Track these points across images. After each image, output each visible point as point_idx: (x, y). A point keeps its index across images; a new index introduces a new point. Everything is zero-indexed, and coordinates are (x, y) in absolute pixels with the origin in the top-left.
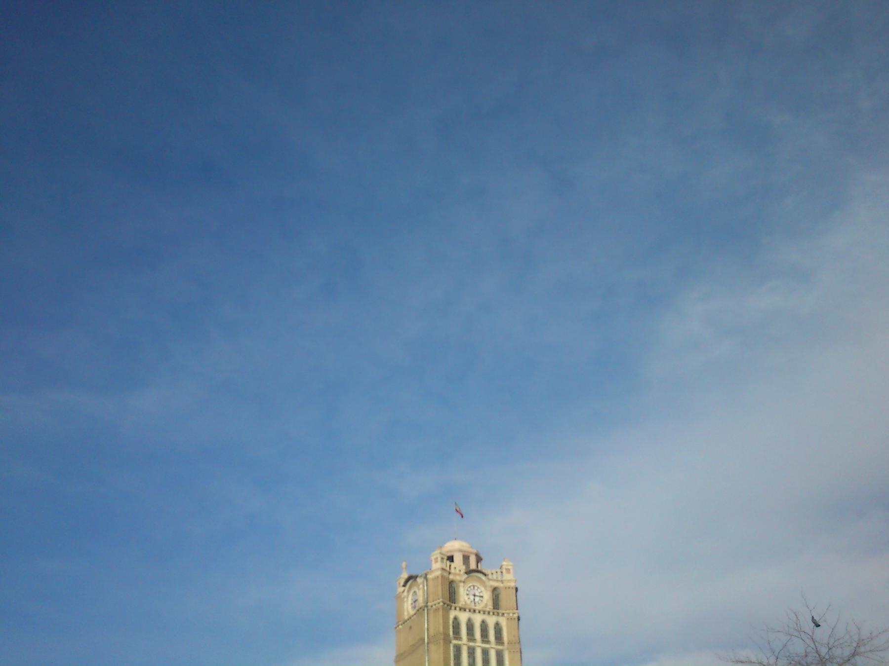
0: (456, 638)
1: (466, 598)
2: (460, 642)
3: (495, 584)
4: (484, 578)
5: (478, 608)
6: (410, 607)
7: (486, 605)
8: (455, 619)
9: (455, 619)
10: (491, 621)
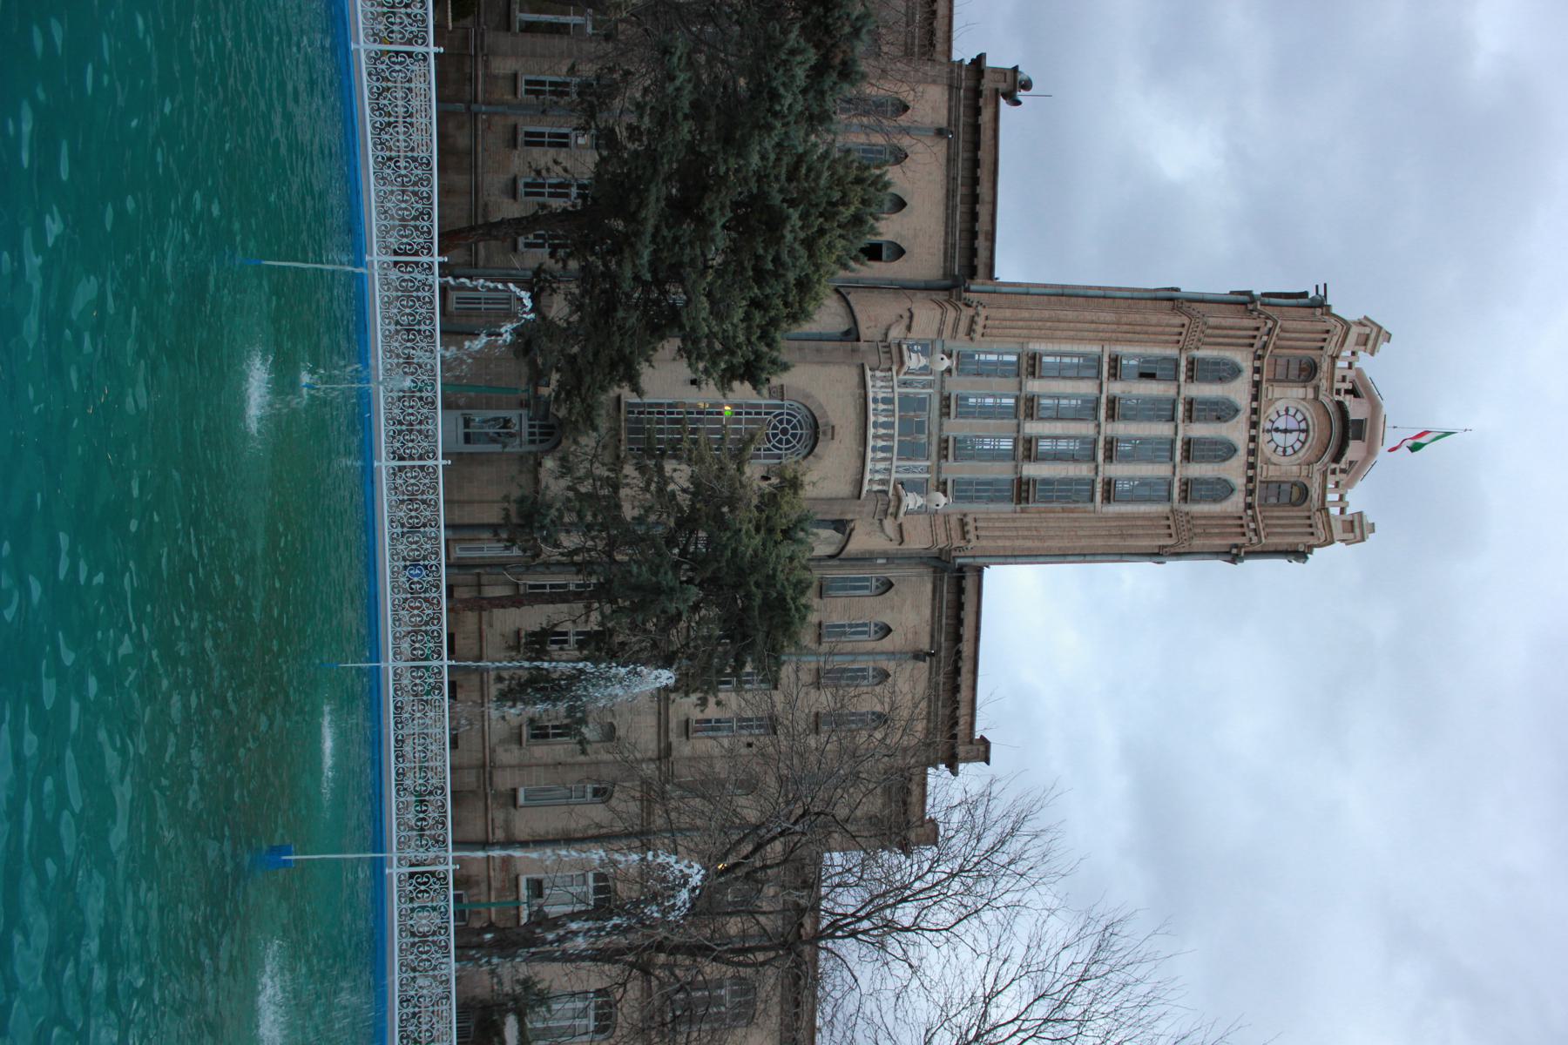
0: (1191, 363)
1: (1281, 406)
2: (1182, 377)
3: (1315, 492)
4: (1326, 458)
7: (1268, 462)
8: (1235, 372)
9: (1235, 372)
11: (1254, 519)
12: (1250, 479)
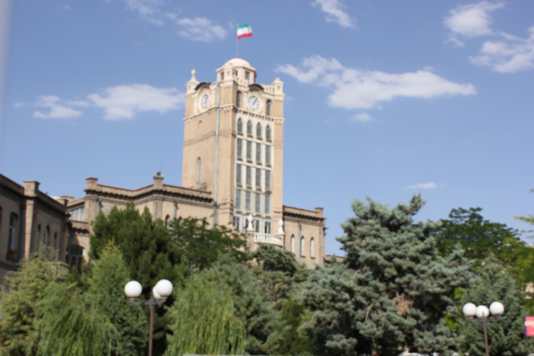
5: (256, 113)
6: (200, 107)
7: (261, 112)
8: (240, 119)
9: (240, 119)
10: (264, 124)
11: (277, 120)
12: (266, 118)
